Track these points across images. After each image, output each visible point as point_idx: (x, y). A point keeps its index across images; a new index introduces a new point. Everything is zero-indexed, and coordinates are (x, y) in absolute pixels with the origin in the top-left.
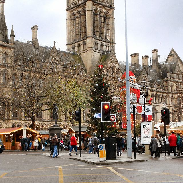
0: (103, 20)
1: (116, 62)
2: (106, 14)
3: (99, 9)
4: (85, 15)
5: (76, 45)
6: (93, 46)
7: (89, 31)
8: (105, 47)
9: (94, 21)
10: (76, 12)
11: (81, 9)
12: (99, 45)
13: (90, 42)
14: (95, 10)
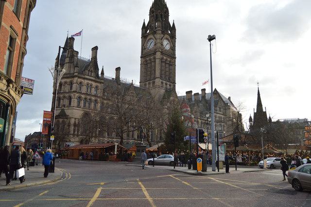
0: (167, 66)
2: (170, 62)
3: (165, 58)
4: (155, 62)
5: (147, 83)
7: (158, 74)
9: (161, 66)
10: (148, 59)
11: (152, 57)
12: (164, 84)
13: (158, 81)
14: (162, 59)
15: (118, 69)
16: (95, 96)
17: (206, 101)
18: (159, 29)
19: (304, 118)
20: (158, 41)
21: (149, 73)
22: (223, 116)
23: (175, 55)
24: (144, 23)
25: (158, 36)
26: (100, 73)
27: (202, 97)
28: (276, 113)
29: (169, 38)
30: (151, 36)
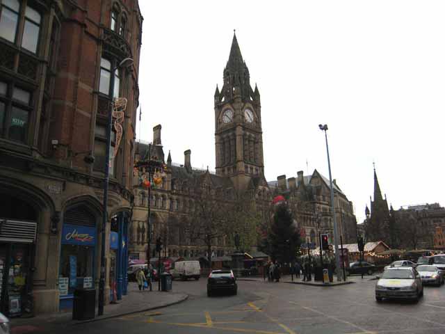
0: (252, 144)
1: (267, 184)
2: (255, 138)
3: (248, 133)
4: (235, 139)
6: (243, 169)
8: (254, 170)
9: (244, 145)
10: (225, 136)
12: (249, 169)
13: (241, 166)
14: (245, 135)
15: (187, 153)
16: (161, 190)
17: (304, 187)
18: (239, 96)
19: (433, 203)
20: (238, 112)
21: (227, 155)
22: (328, 207)
23: (260, 128)
24: (217, 89)
25: (236, 106)
26: (166, 159)
27: (299, 183)
28: (398, 201)
29: (252, 108)
30: (228, 106)
